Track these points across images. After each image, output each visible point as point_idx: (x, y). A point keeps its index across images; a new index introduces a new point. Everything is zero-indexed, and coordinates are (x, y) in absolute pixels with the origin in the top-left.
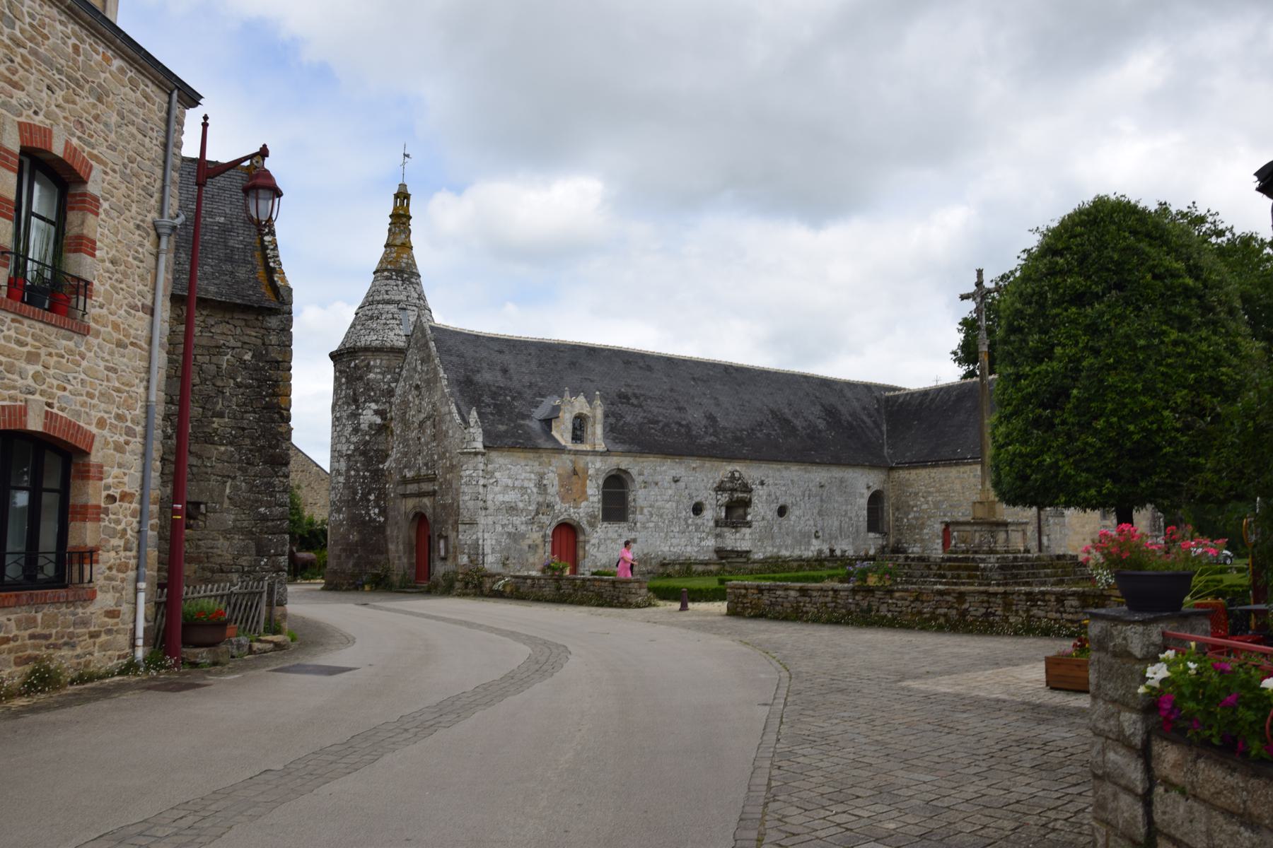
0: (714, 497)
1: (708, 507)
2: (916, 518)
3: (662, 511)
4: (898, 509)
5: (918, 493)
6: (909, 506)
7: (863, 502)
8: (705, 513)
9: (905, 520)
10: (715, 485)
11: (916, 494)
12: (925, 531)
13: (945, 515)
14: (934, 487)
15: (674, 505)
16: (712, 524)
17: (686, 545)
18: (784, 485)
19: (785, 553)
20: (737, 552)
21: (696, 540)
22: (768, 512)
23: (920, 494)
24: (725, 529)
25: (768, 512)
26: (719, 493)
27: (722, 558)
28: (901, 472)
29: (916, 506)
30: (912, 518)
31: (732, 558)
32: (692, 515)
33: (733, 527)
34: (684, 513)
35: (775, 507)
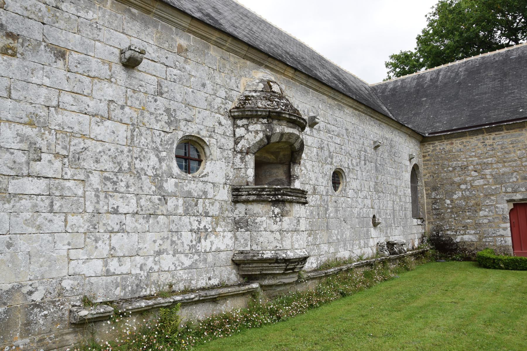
0: (229, 132)
1: (215, 152)
2: (464, 198)
3: (77, 144)
4: (435, 189)
5: (466, 167)
6: (453, 183)
7: (407, 176)
8: (207, 167)
9: (448, 202)
10: (230, 106)
11: (464, 168)
12: (481, 213)
13: (515, 191)
14: (492, 156)
15: (123, 131)
16: (225, 194)
17: (159, 253)
18: (338, 135)
19: (344, 254)
20: (287, 261)
21: (187, 237)
22: (321, 180)
23: (471, 167)
24: (257, 208)
25: (321, 180)
26: (239, 122)
27: (249, 278)
28: (437, 143)
29: (466, 183)
30: (459, 199)
31: (274, 275)
32: (176, 170)
33: (275, 203)
34: (153, 160)
35: (329, 170)
